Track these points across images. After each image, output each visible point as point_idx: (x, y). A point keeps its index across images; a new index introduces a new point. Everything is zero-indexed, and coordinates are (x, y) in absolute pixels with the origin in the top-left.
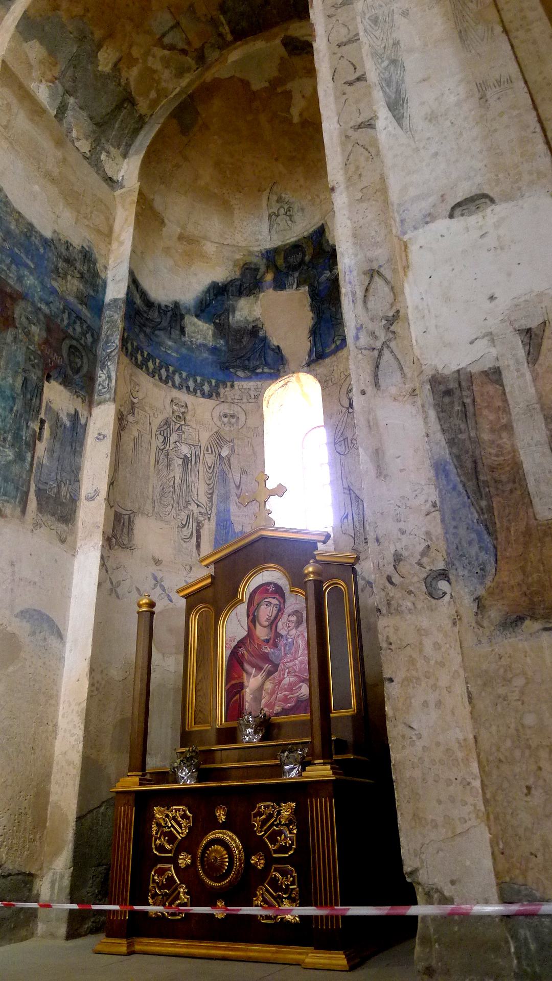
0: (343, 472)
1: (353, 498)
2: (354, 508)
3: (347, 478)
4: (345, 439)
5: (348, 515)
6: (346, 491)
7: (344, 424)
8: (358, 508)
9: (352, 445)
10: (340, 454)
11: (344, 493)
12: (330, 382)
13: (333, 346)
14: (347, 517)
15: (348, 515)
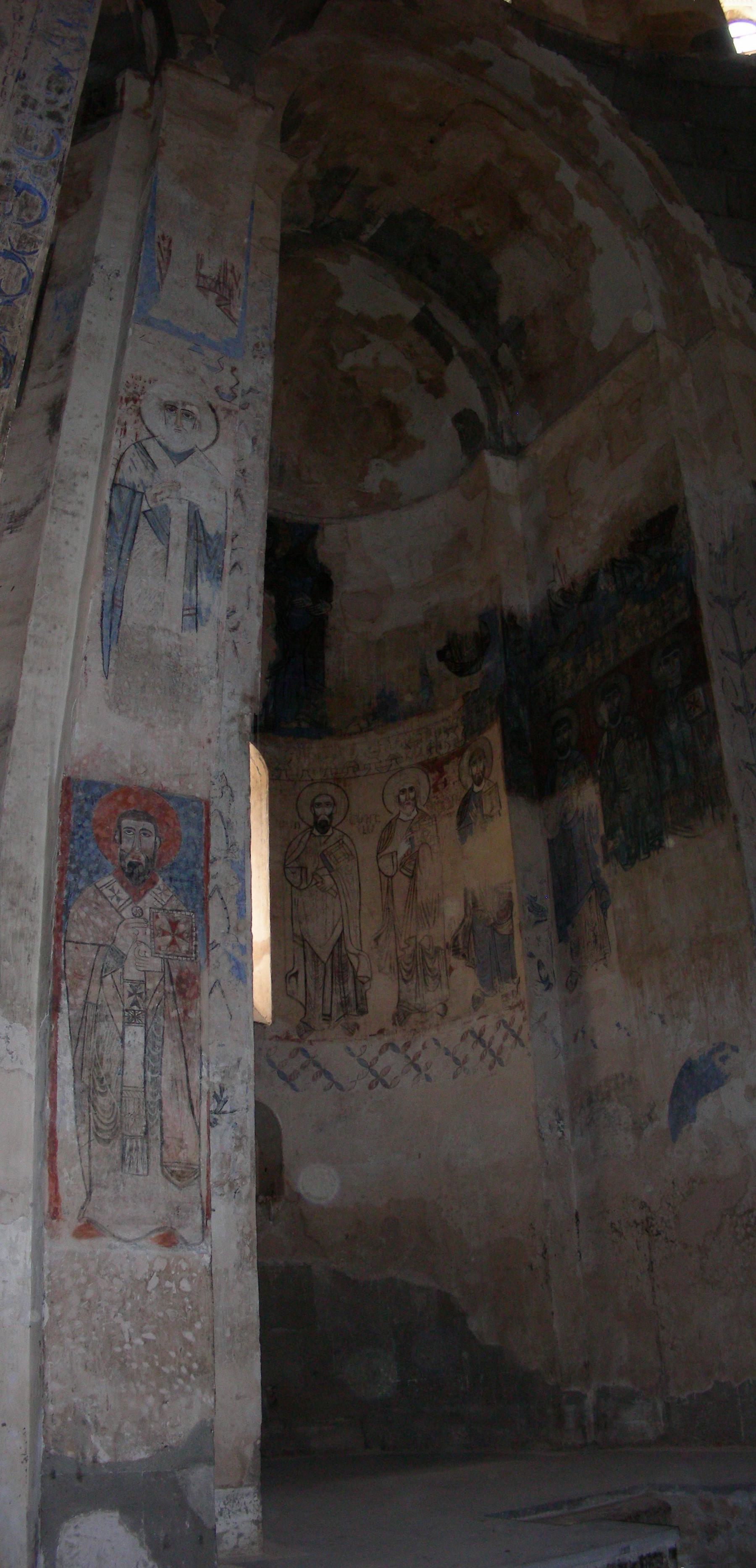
0: (294, 910)
1: (309, 954)
2: (310, 970)
3: (300, 923)
4: (303, 868)
5: (297, 973)
6: (296, 939)
7: (302, 846)
8: (317, 971)
9: (314, 882)
10: (292, 885)
11: (294, 941)
12: (283, 773)
13: (294, 725)
14: (296, 975)
15: (297, 973)
